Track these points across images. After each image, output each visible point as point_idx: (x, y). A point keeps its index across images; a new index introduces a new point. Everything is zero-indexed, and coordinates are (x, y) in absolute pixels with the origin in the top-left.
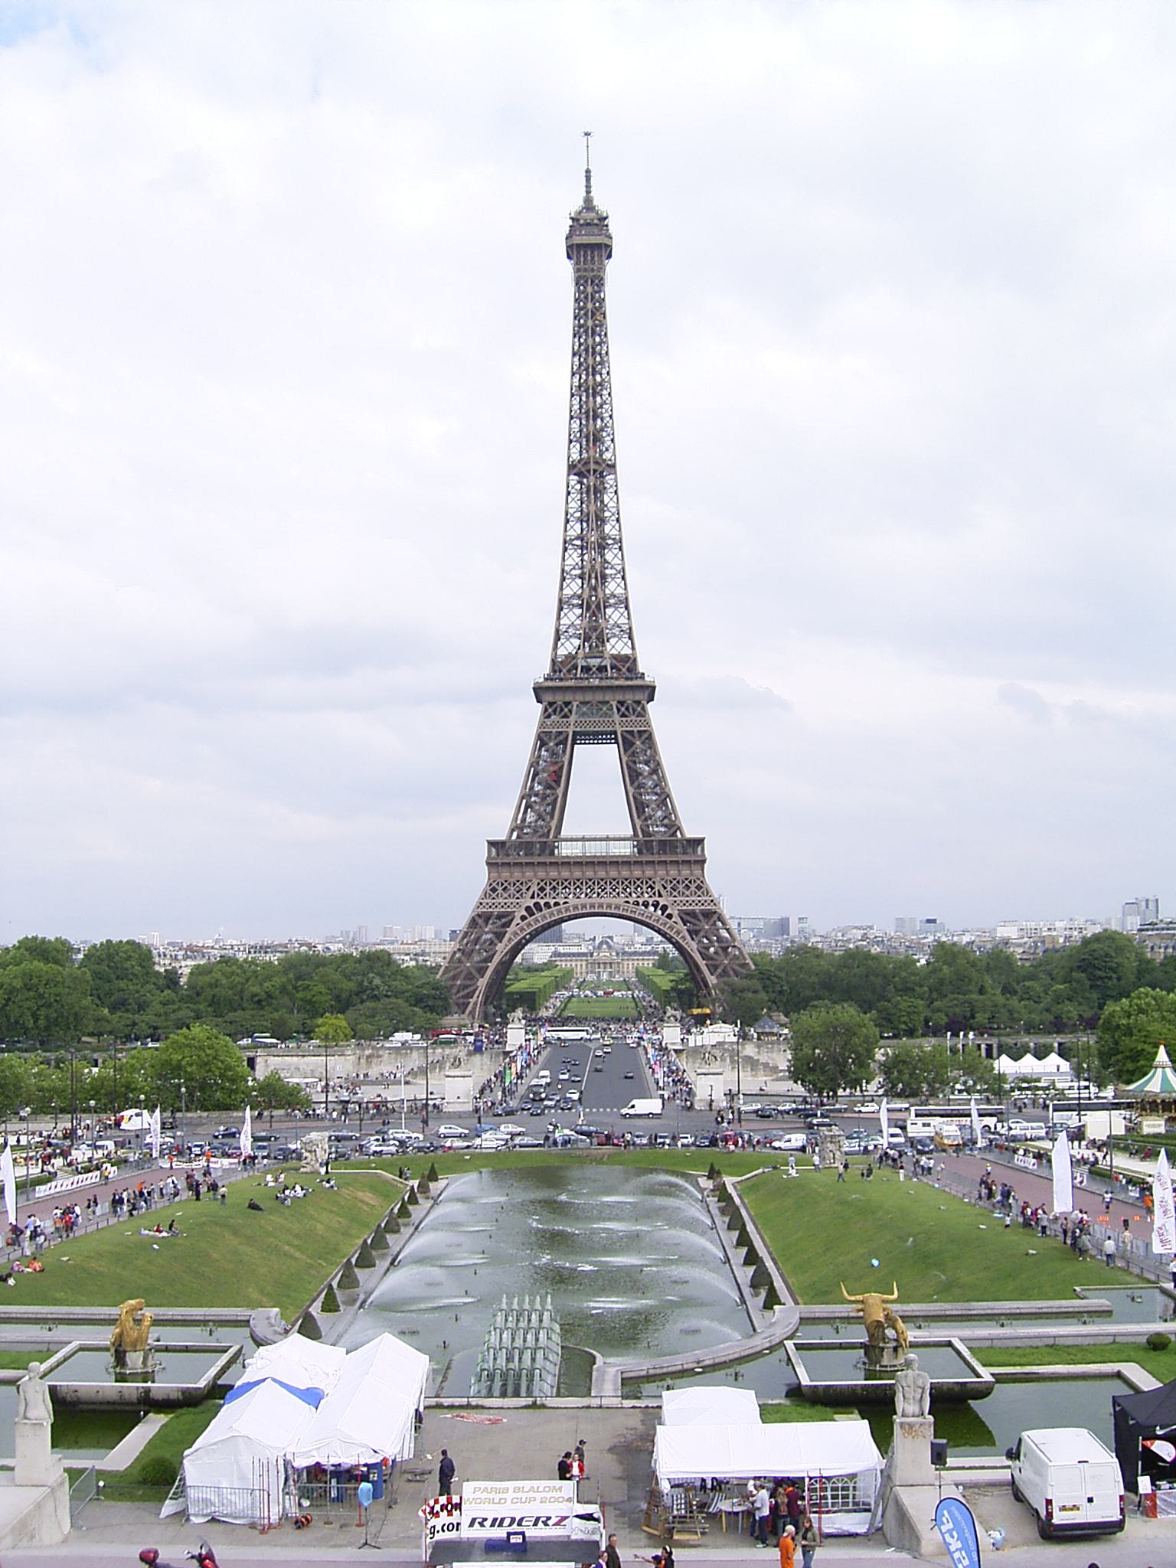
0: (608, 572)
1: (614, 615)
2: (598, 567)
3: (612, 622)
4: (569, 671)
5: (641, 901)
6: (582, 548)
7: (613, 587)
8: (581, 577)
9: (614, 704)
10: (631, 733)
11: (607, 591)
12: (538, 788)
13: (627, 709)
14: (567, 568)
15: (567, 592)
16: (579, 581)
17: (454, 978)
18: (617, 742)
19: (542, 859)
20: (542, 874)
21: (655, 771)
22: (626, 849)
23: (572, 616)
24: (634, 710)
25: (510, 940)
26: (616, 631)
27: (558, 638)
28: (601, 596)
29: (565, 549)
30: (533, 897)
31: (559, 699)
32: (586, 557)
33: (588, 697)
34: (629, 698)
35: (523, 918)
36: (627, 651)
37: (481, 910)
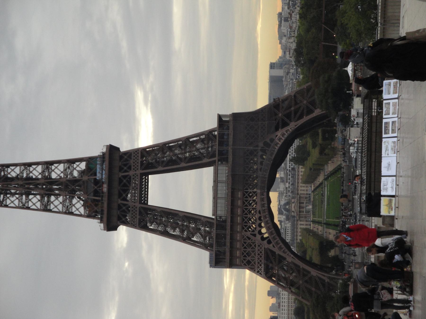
0: (25, 175)
1: (57, 172)
2: (21, 183)
3: (62, 175)
4: (96, 205)
5: (260, 160)
6: (6, 194)
7: (36, 172)
8: (28, 194)
9: (121, 174)
10: (142, 162)
11: (40, 177)
12: (177, 232)
13: (125, 165)
14: (21, 205)
15: (38, 205)
16: (31, 197)
17: (310, 292)
18: (147, 174)
19: (228, 228)
20: (239, 228)
21: (170, 149)
22: (224, 170)
23: (57, 202)
24: (127, 160)
25: (284, 252)
26: (69, 171)
27: (72, 213)
28: (43, 181)
29: (6, 206)
30: (255, 235)
31: (115, 212)
32: (13, 191)
33: (116, 192)
34: (117, 163)
35: (269, 242)
36: (83, 166)
37: (263, 273)
